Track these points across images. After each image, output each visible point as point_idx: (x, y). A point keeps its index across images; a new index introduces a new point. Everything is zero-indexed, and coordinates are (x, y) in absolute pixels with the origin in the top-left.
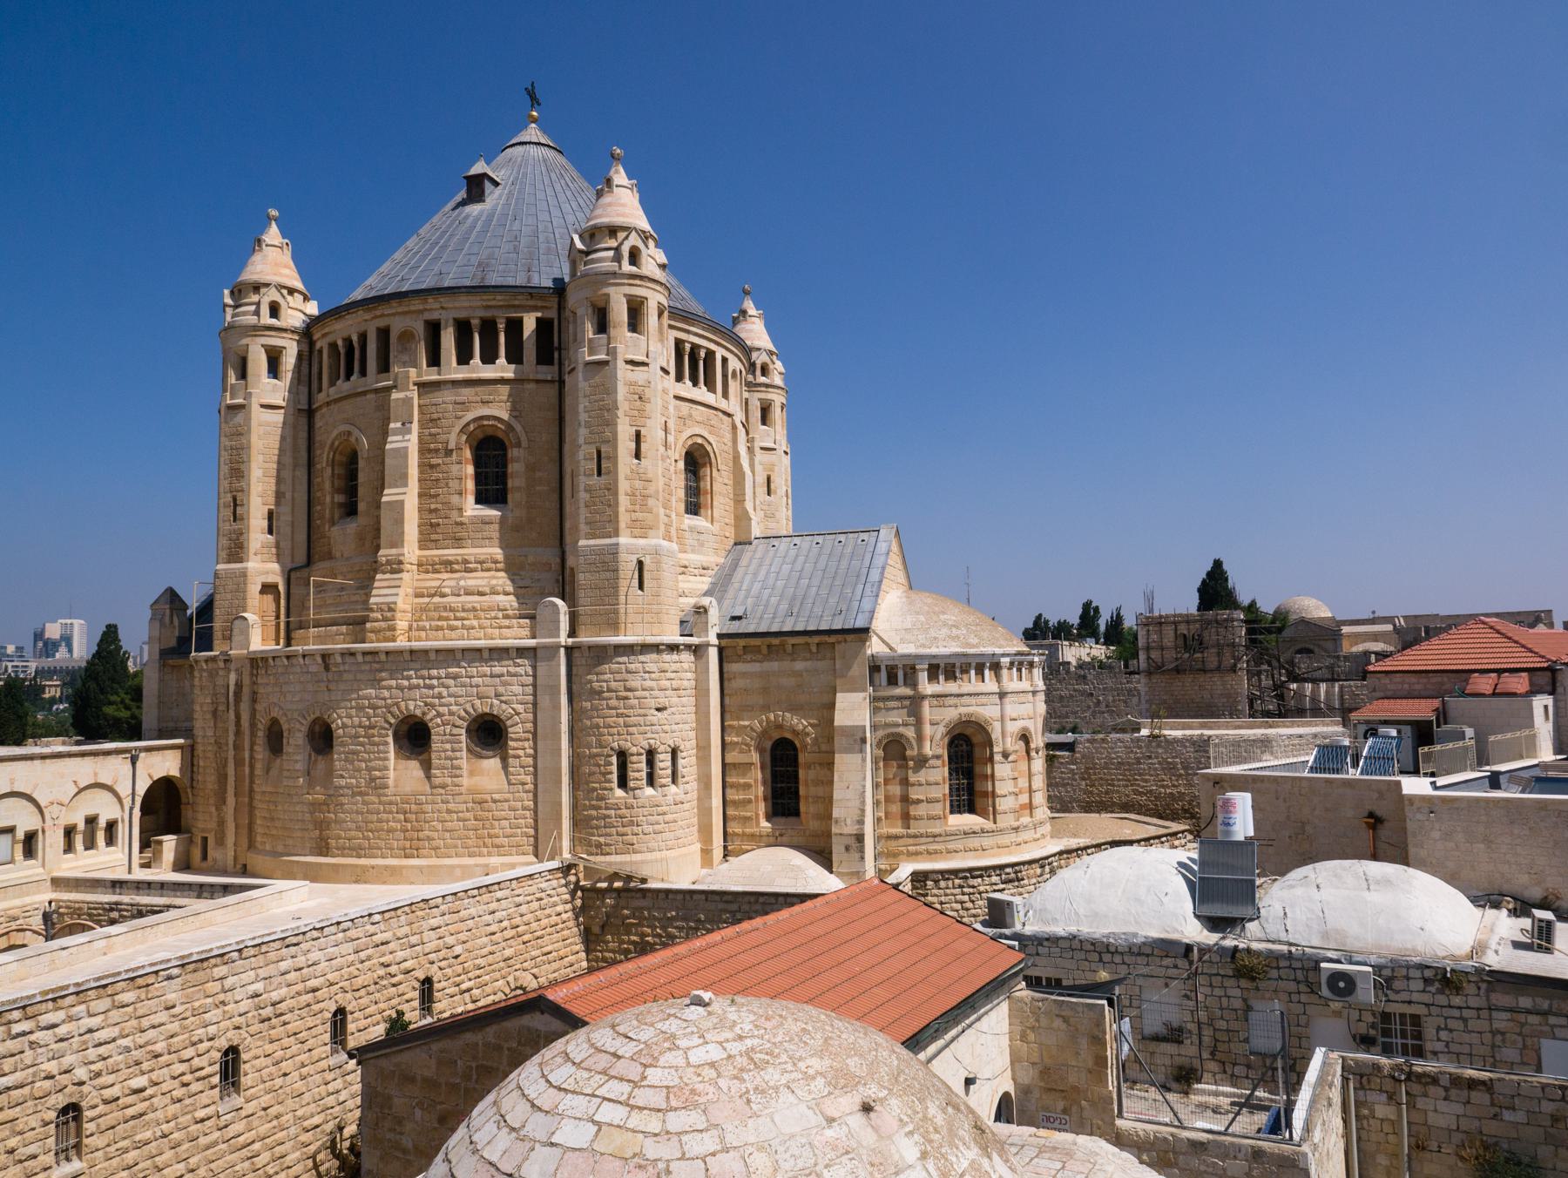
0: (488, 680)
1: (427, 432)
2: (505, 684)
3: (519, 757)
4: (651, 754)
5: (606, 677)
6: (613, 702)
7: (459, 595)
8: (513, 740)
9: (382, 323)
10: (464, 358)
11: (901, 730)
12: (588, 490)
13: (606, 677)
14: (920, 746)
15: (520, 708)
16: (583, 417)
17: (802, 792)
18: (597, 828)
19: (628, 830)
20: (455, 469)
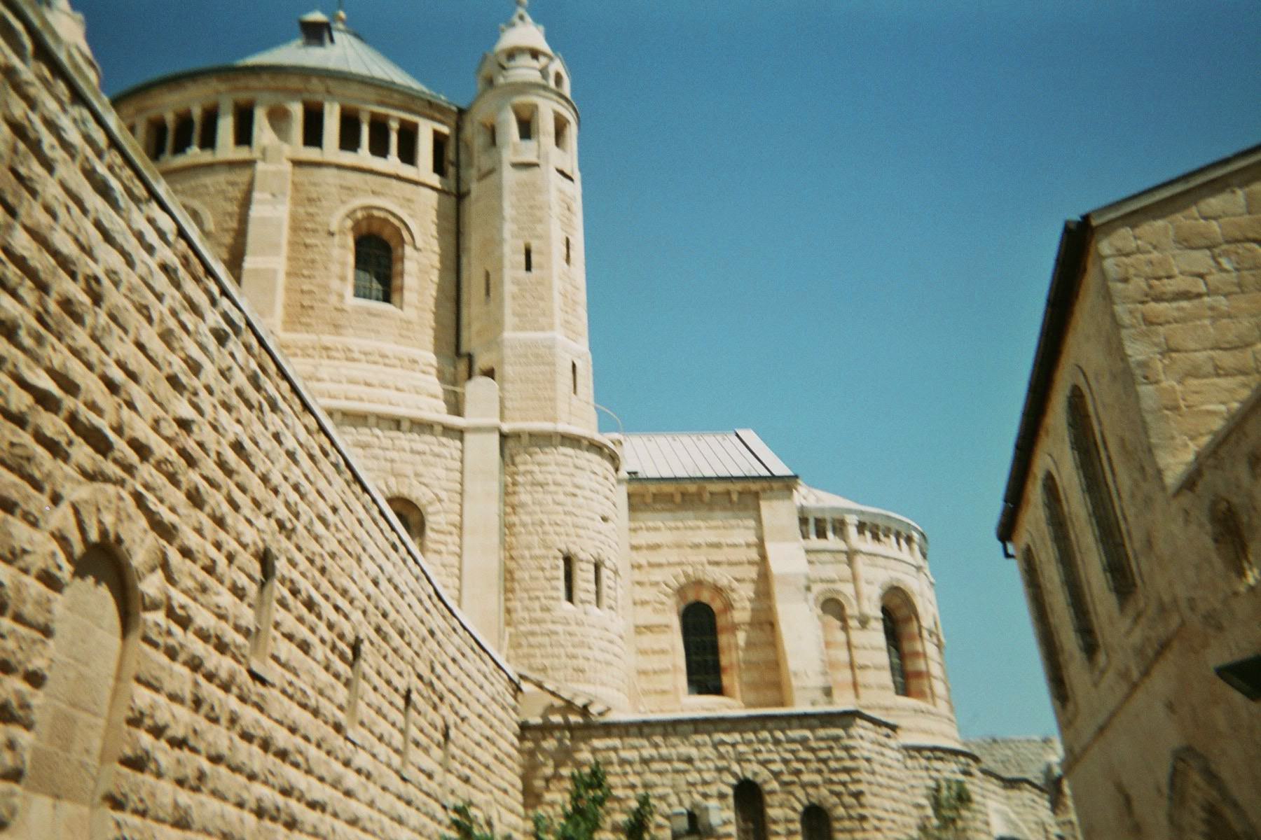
0: (408, 456)
1: (301, 210)
2: (426, 464)
3: (439, 552)
4: (597, 567)
5: (550, 468)
6: (561, 498)
7: (340, 382)
8: (433, 530)
9: (243, 96)
10: (349, 140)
11: (839, 586)
12: (517, 282)
13: (550, 468)
14: (859, 604)
15: (443, 495)
16: (508, 211)
17: (724, 660)
18: (541, 646)
19: (578, 651)
20: (336, 252)
